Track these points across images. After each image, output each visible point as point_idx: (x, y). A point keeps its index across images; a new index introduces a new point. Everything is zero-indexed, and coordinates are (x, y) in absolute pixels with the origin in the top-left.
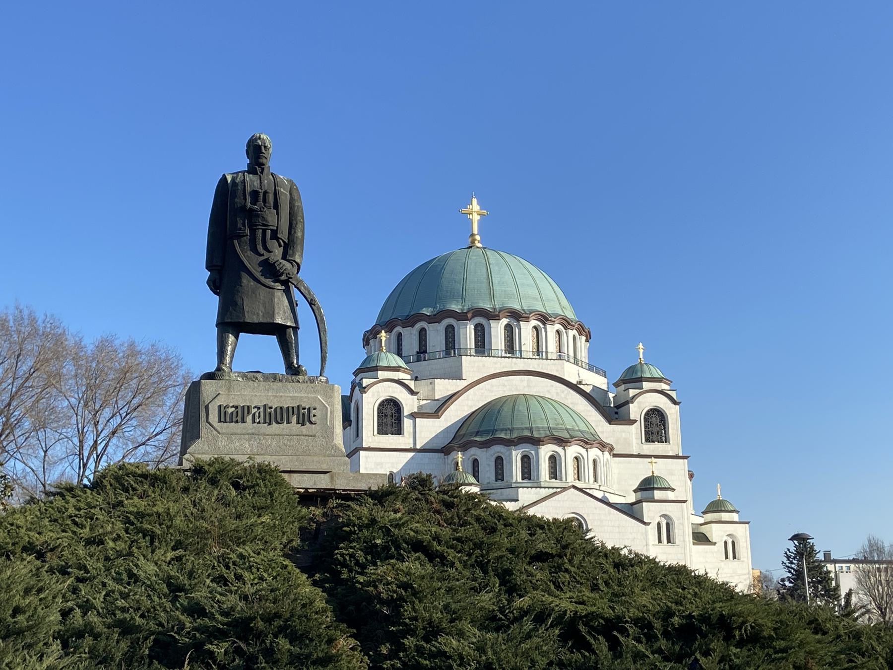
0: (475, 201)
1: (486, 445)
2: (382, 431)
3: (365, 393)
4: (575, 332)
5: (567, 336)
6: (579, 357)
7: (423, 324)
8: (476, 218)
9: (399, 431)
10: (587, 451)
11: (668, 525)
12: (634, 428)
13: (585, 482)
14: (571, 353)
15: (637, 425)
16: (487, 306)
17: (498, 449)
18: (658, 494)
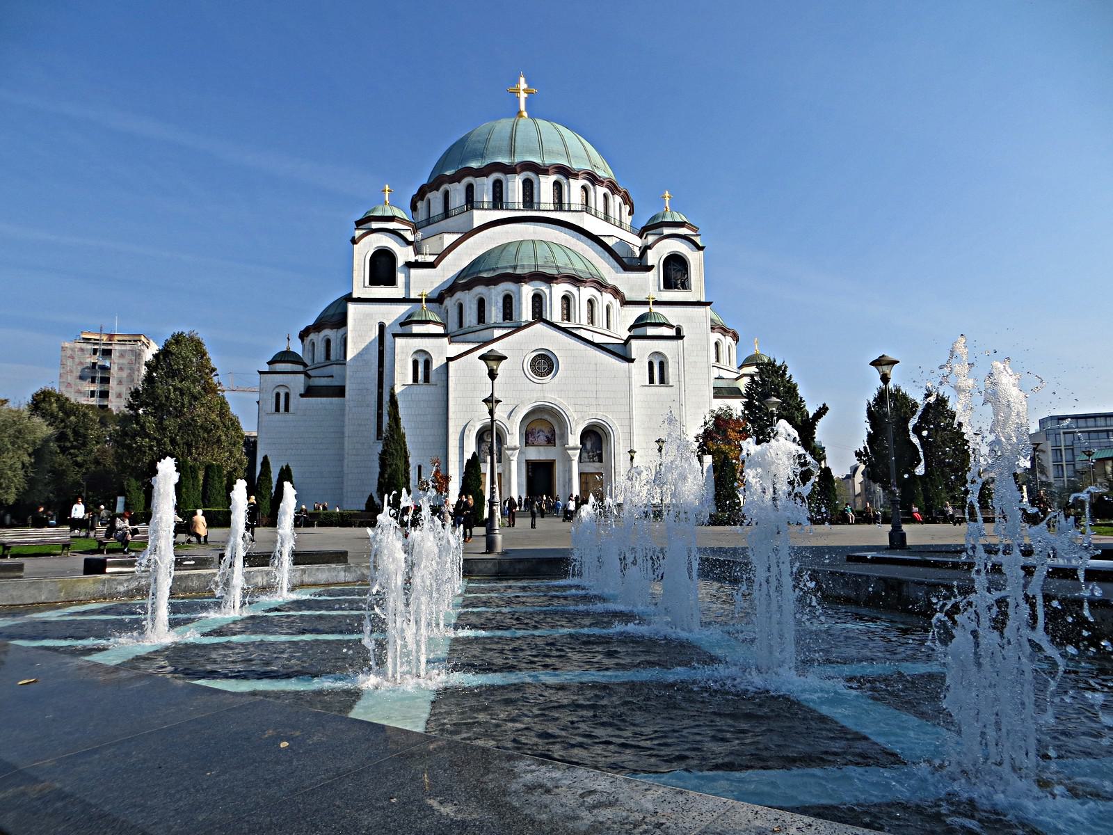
0: (522, 80)
1: (468, 287)
2: (375, 280)
3: (356, 243)
4: (606, 190)
5: (595, 193)
6: (611, 213)
7: (445, 186)
8: (523, 96)
9: (391, 282)
10: (579, 290)
11: (662, 365)
12: (651, 275)
13: (575, 321)
14: (601, 208)
15: (654, 271)
16: (505, 160)
17: (480, 290)
18: (651, 331)
